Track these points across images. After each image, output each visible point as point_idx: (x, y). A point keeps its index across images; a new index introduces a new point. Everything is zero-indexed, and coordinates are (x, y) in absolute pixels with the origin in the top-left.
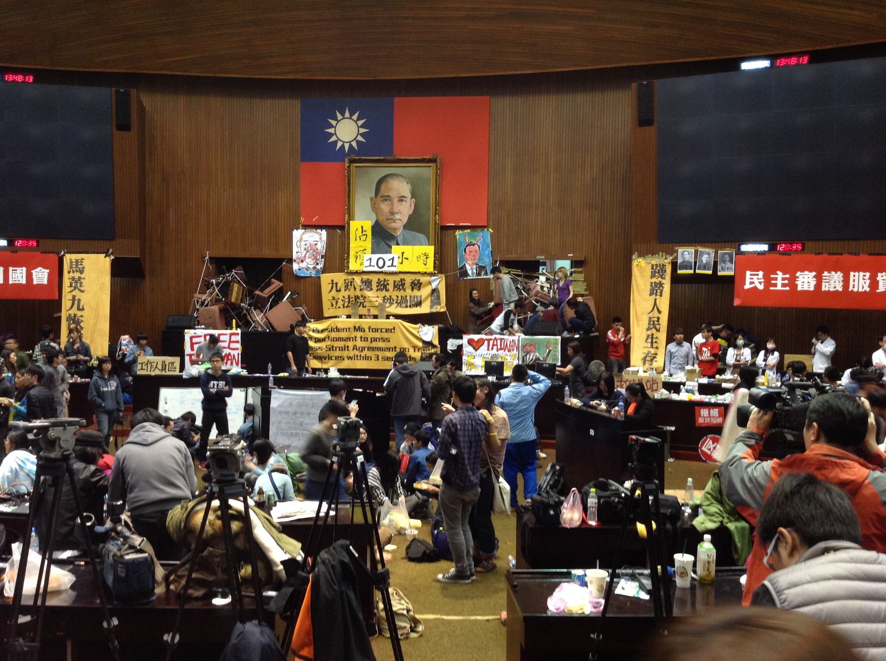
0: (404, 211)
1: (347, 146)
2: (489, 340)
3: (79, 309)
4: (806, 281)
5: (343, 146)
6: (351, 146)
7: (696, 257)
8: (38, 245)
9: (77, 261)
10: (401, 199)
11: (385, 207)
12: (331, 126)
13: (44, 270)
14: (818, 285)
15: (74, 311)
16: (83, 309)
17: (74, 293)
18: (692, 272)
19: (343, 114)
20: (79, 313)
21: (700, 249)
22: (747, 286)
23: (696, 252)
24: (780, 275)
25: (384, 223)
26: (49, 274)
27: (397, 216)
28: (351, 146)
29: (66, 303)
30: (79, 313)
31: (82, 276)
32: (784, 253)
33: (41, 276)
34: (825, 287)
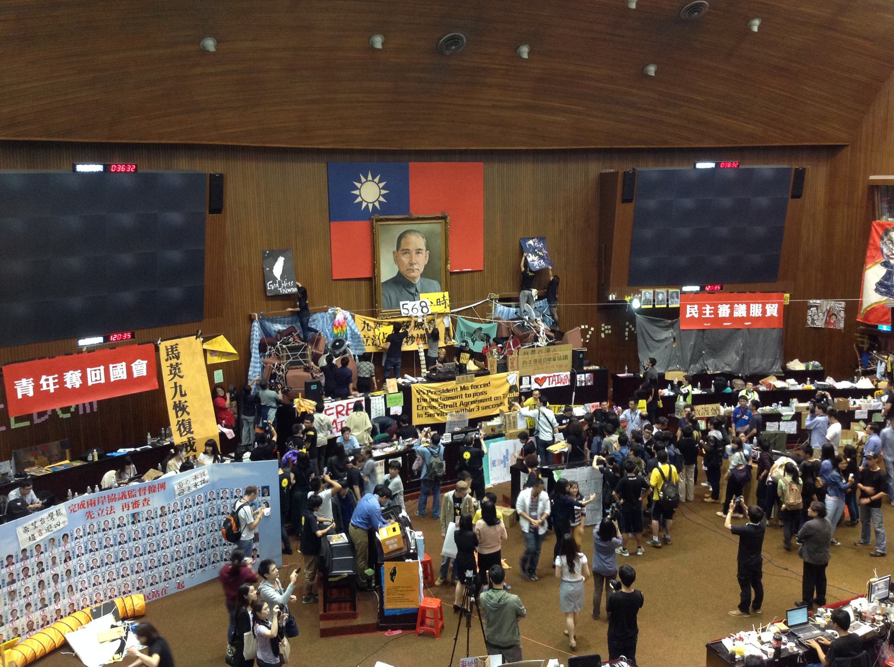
0: (421, 261)
1: (371, 206)
2: (549, 377)
3: (182, 395)
4: (724, 311)
5: (367, 206)
6: (374, 206)
7: (654, 296)
8: (133, 336)
9: (172, 347)
10: (418, 251)
11: (405, 259)
12: (356, 188)
13: (142, 362)
14: (731, 314)
15: (178, 398)
16: (185, 395)
17: (175, 380)
18: (651, 306)
19: (366, 177)
20: (183, 399)
21: (657, 290)
22: (688, 316)
23: (654, 292)
24: (708, 307)
25: (405, 273)
26: (147, 365)
27: (416, 267)
28: (374, 206)
29: (169, 392)
30: (183, 399)
31: (179, 361)
32: (710, 292)
33: (140, 368)
34: (736, 315)
